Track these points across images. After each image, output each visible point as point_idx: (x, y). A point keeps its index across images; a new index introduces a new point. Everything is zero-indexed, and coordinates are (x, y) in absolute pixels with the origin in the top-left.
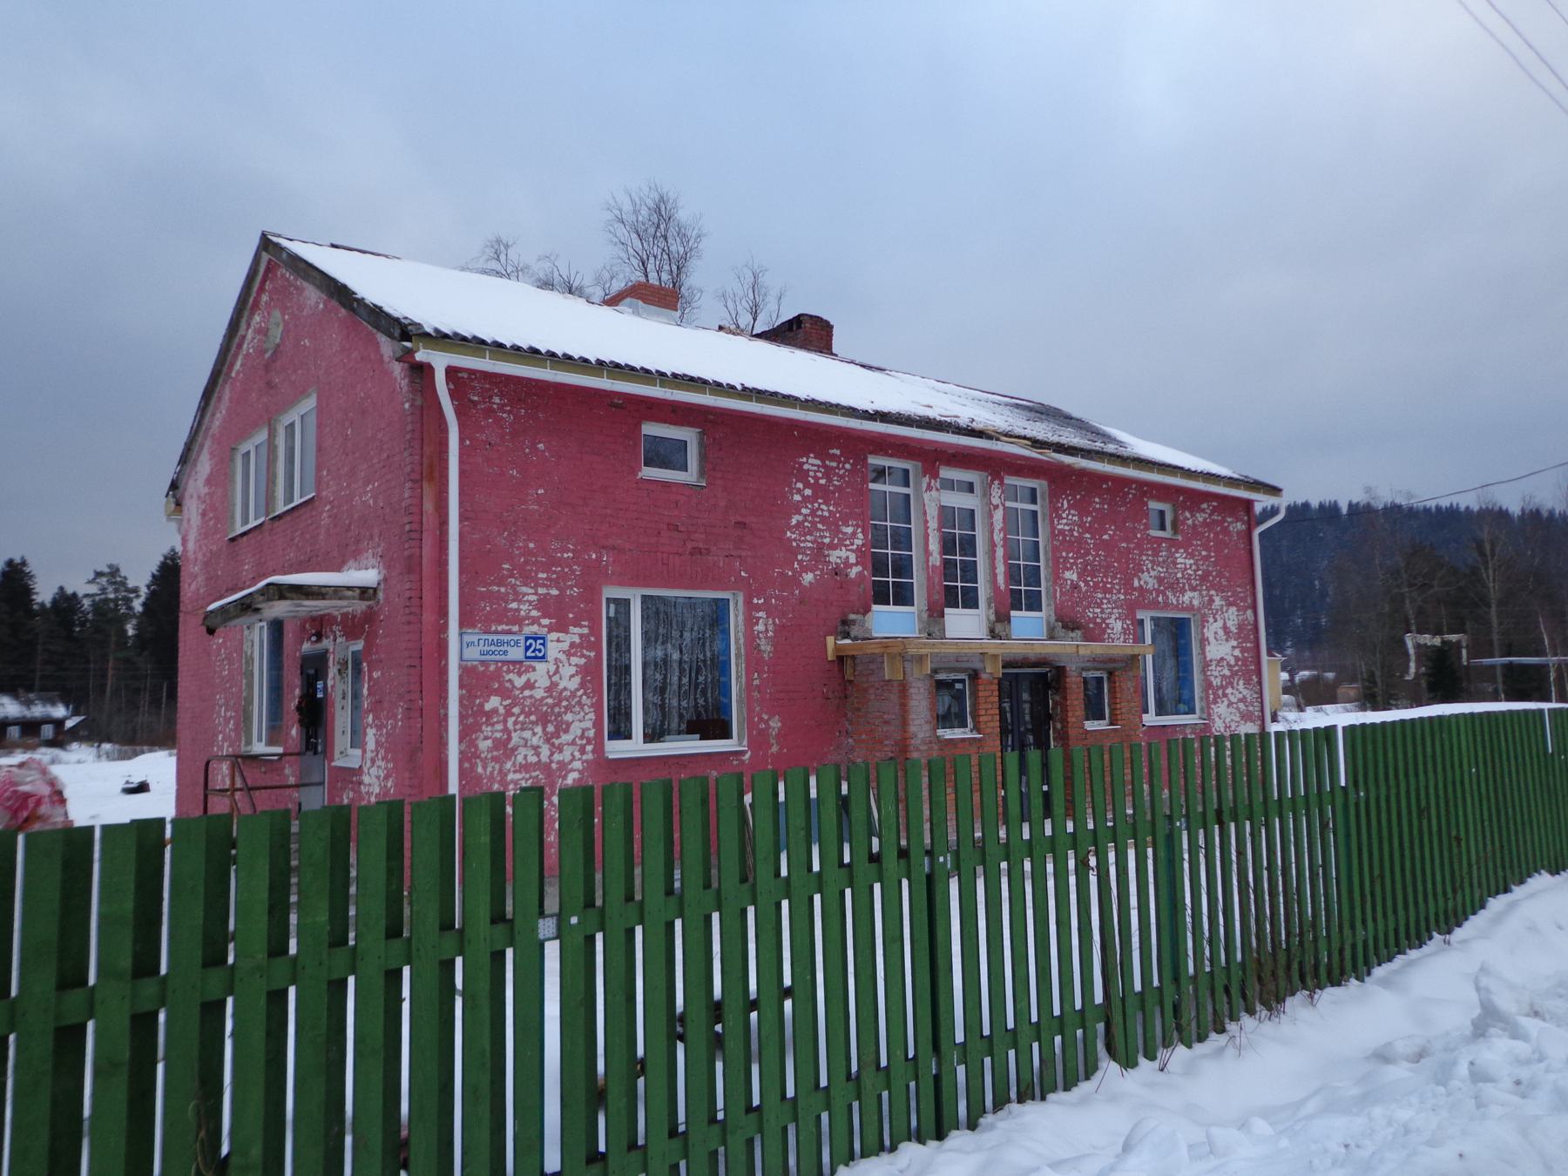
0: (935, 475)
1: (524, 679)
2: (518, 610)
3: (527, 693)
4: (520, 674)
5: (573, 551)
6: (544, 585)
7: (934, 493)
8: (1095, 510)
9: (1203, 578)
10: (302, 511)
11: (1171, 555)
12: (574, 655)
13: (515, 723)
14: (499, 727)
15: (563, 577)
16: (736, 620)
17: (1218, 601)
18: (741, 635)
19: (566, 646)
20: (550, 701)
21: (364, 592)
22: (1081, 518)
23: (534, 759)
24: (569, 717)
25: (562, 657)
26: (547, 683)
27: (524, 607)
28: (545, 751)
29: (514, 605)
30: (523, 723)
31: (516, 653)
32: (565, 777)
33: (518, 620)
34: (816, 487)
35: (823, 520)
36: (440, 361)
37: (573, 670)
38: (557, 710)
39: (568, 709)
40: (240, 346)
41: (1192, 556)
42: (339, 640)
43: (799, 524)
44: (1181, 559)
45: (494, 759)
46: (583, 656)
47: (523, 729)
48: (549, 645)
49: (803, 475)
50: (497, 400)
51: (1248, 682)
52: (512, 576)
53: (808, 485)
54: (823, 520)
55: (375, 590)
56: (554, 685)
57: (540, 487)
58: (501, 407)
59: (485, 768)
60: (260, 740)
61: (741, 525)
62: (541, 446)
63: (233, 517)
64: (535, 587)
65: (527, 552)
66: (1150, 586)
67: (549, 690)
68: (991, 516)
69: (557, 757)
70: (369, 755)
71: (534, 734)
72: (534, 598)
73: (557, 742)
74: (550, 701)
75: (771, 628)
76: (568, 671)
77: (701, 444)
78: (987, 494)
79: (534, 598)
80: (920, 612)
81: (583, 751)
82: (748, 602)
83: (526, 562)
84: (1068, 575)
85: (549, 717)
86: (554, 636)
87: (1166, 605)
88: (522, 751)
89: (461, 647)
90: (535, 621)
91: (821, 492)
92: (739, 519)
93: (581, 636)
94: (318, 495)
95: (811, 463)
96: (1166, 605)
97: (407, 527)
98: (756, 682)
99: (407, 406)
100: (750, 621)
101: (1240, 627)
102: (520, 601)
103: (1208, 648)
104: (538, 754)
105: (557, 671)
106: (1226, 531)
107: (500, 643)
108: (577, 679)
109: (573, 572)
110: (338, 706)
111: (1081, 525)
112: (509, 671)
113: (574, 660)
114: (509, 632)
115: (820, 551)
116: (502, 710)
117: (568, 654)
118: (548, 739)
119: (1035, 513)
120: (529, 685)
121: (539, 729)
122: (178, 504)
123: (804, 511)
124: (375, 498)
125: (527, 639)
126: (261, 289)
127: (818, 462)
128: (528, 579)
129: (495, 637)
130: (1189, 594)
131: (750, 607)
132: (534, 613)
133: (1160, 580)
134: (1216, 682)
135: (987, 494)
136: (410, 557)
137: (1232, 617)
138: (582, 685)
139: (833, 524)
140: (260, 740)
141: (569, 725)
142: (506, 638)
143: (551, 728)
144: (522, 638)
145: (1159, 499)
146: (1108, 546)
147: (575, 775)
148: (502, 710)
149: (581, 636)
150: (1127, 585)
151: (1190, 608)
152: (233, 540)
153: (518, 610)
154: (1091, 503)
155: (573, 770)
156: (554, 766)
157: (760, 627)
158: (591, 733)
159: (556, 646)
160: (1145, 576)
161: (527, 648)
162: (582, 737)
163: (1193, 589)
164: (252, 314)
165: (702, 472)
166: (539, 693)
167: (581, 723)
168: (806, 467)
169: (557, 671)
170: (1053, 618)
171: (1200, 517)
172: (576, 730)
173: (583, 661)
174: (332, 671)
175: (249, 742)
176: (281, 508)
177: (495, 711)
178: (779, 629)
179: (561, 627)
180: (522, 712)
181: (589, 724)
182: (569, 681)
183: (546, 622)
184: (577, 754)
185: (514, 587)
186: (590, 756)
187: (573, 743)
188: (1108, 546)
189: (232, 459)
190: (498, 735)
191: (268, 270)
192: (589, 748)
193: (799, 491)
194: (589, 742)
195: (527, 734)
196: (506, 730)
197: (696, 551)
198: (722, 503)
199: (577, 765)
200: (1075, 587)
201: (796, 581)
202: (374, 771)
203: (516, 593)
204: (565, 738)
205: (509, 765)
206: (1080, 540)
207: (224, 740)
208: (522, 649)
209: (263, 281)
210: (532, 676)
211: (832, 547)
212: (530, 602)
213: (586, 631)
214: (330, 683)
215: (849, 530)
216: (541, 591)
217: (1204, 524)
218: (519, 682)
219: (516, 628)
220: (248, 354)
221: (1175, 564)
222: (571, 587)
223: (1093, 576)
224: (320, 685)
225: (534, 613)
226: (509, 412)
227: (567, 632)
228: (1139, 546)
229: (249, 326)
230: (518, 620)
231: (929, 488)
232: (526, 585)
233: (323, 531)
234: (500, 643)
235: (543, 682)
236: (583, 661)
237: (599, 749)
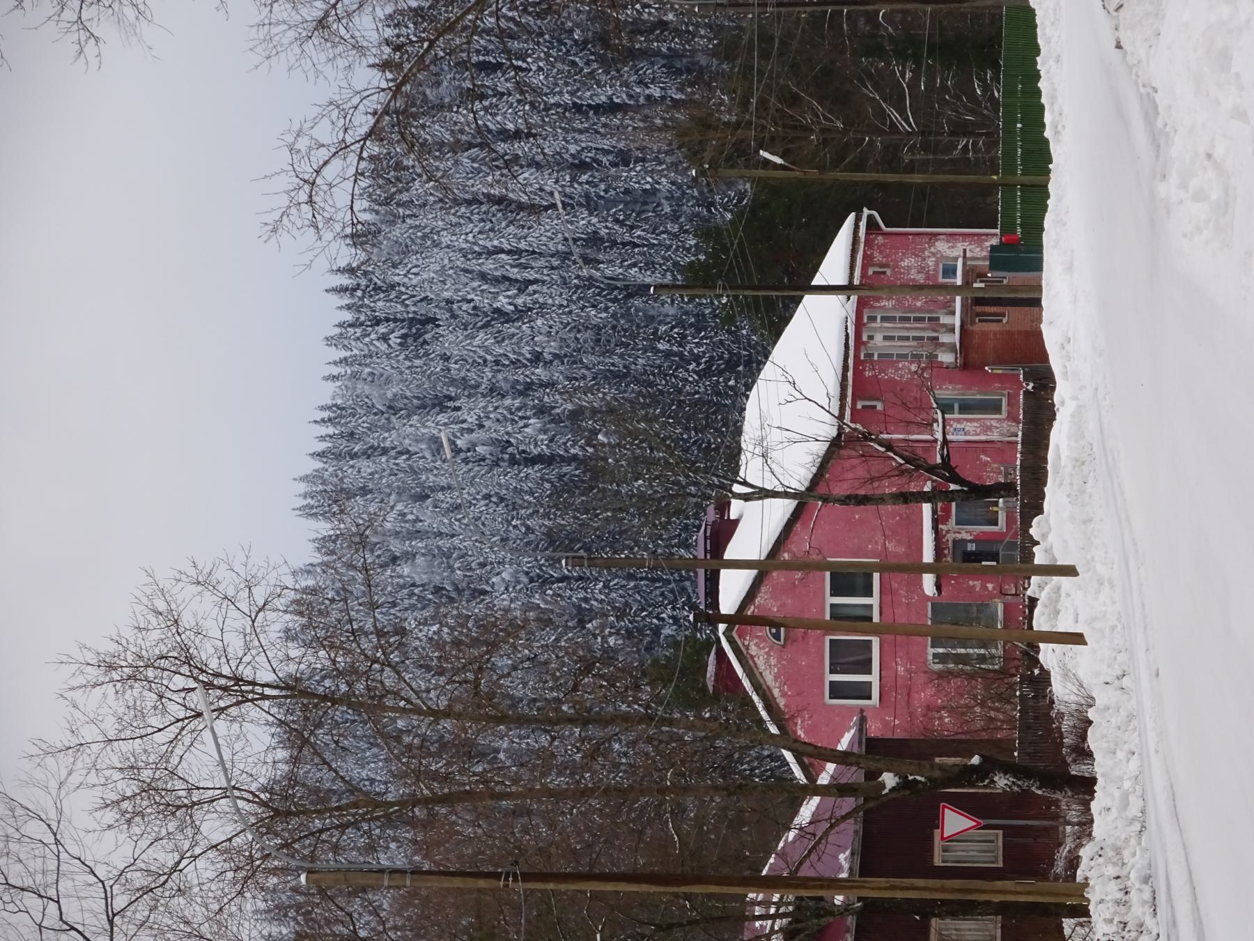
9: (917, 256)
44: (905, 263)
78: (875, 329)
101: (948, 242)
106: (884, 245)
126: (747, 648)
131: (941, 388)
133: (919, 272)
137: (942, 246)
139: (897, 369)
171: (876, 254)
214: (969, 538)
217: (881, 253)
220: (776, 678)
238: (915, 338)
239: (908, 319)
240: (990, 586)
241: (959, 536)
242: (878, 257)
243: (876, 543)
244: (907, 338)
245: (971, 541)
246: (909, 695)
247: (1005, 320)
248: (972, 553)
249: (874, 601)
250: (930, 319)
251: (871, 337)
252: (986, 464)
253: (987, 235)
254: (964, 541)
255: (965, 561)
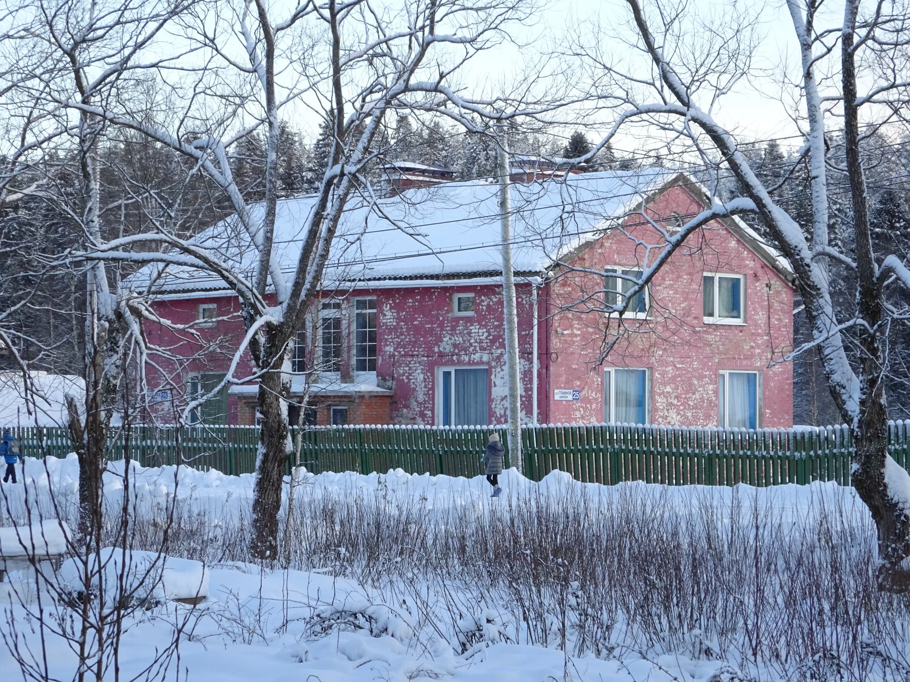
8: (409, 307)
9: (493, 342)
22: (398, 313)
41: (485, 326)
44: (474, 329)
66: (447, 351)
84: (387, 348)
87: (460, 362)
96: (460, 362)
103: (493, 389)
111: (399, 319)
120: (163, 410)
146: (417, 330)
154: (405, 303)
163: (483, 349)
200: (394, 356)
221: (469, 334)
223: (404, 347)
228: (441, 326)
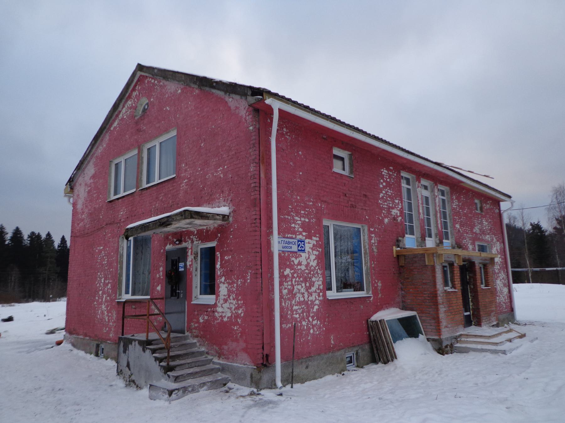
0: (420, 182)
1: (298, 260)
2: (295, 228)
3: (299, 267)
4: (296, 258)
5: (313, 202)
6: (303, 217)
7: (419, 189)
9: (490, 230)
10: (166, 184)
11: (481, 221)
12: (314, 250)
13: (295, 281)
14: (290, 283)
15: (309, 213)
16: (364, 237)
17: (495, 240)
18: (367, 244)
19: (311, 245)
20: (307, 271)
21: (224, 217)
23: (302, 299)
24: (314, 279)
25: (311, 251)
26: (306, 263)
27: (297, 226)
28: (306, 295)
29: (293, 225)
30: (298, 282)
31: (295, 248)
32: (313, 308)
33: (294, 233)
34: (386, 182)
35: (390, 197)
36: (276, 105)
37: (314, 257)
38: (309, 276)
39: (313, 275)
40: (117, 116)
42: (195, 243)
43: (383, 197)
45: (289, 299)
46: (317, 251)
47: (298, 285)
48: (306, 245)
49: (382, 177)
50: (285, 130)
51: (504, 271)
52: (292, 211)
53: (384, 181)
54: (390, 197)
55: (228, 216)
56: (308, 264)
57: (301, 171)
58: (287, 133)
59: (285, 304)
60: (127, 292)
61: (365, 196)
62: (300, 153)
63: (110, 192)
64: (300, 218)
65: (297, 201)
67: (307, 265)
68: (435, 200)
69: (310, 298)
70: (222, 297)
71: (302, 287)
72: (299, 222)
73: (310, 291)
74: (307, 271)
75: (376, 241)
76: (313, 257)
77: (350, 159)
78: (433, 191)
79: (299, 222)
80: (417, 238)
81: (319, 296)
82: (369, 230)
83: (297, 205)
85: (307, 279)
86: (307, 241)
88: (298, 295)
89: (277, 244)
90: (301, 233)
91: (388, 185)
92: (365, 193)
93: (317, 241)
94: (178, 176)
95: (385, 172)
97: (253, 185)
98: (373, 265)
99: (251, 128)
100: (370, 238)
101: (501, 249)
102: (295, 223)
104: (304, 297)
105: (309, 258)
106: (494, 212)
107: (289, 243)
108: (316, 261)
109: (313, 211)
110: (194, 274)
111: (459, 206)
112: (293, 257)
113: (315, 252)
114: (292, 238)
115: (389, 209)
116: (290, 275)
117: (313, 249)
118: (307, 289)
119: (443, 200)
120: (300, 264)
121: (303, 285)
122: (72, 188)
123: (384, 192)
124: (225, 174)
125: (298, 241)
126: (134, 90)
127: (386, 172)
128: (298, 214)
129: (287, 240)
130: (488, 236)
131: (370, 232)
132: (300, 230)
133: (480, 230)
134: (497, 271)
135: (433, 191)
136: (255, 199)
138: (318, 264)
140: (127, 292)
141: (314, 282)
142: (291, 240)
143: (308, 285)
144: (296, 241)
145: (478, 198)
147: (316, 307)
148: (290, 275)
149: (317, 241)
150: (472, 231)
151: (487, 242)
152: (110, 202)
153: (295, 228)
155: (316, 305)
156: (309, 302)
157: (373, 241)
158: (321, 287)
159: (308, 247)
160: (476, 228)
161: (299, 246)
162: (319, 289)
163: (488, 234)
164: (126, 101)
165: (351, 172)
166: (303, 268)
167: (318, 282)
168: (383, 173)
169: (309, 258)
170: (454, 243)
171: (488, 206)
172: (316, 284)
173: (317, 253)
174: (190, 258)
175: (120, 295)
176: (145, 186)
177: (288, 275)
178: (379, 242)
179: (309, 237)
180: (298, 276)
181: (320, 283)
182: (314, 263)
183: (304, 234)
184: (317, 297)
185: (293, 216)
186: (321, 298)
187: (315, 292)
188: (465, 215)
189: (110, 166)
190: (289, 287)
191: (138, 80)
192: (321, 294)
193: (382, 183)
194: (321, 292)
195: (299, 287)
196: (293, 286)
197: (352, 206)
198: (359, 186)
199: (317, 302)
201: (382, 222)
202: (226, 305)
203: (294, 219)
204: (313, 289)
205: (293, 302)
206: (459, 212)
207: (103, 294)
208: (297, 246)
209: (135, 86)
210: (300, 259)
211: (393, 208)
212: (299, 224)
213: (318, 239)
214: (188, 263)
215: (397, 201)
216: (303, 219)
218: (296, 262)
219: (294, 236)
220: (122, 119)
222: (312, 218)
224: (181, 264)
225: (300, 230)
226: (289, 136)
227: (312, 239)
229: (124, 106)
230: (294, 233)
231: (418, 187)
232: (297, 216)
233: (182, 192)
234: (289, 243)
235: (304, 263)
236: (317, 253)
237: (324, 295)
238: (429, 220)
239: (445, 218)
240: (159, 288)
241: (189, 254)
242: (487, 206)
243: (186, 171)
244: (428, 214)
245: (185, 266)
246: (110, 224)
247: (449, 289)
248: (178, 268)
249: (157, 181)
250: (447, 233)
251: (426, 188)
252: (244, 278)
253: (507, 272)
254: (185, 261)
255: (173, 261)
